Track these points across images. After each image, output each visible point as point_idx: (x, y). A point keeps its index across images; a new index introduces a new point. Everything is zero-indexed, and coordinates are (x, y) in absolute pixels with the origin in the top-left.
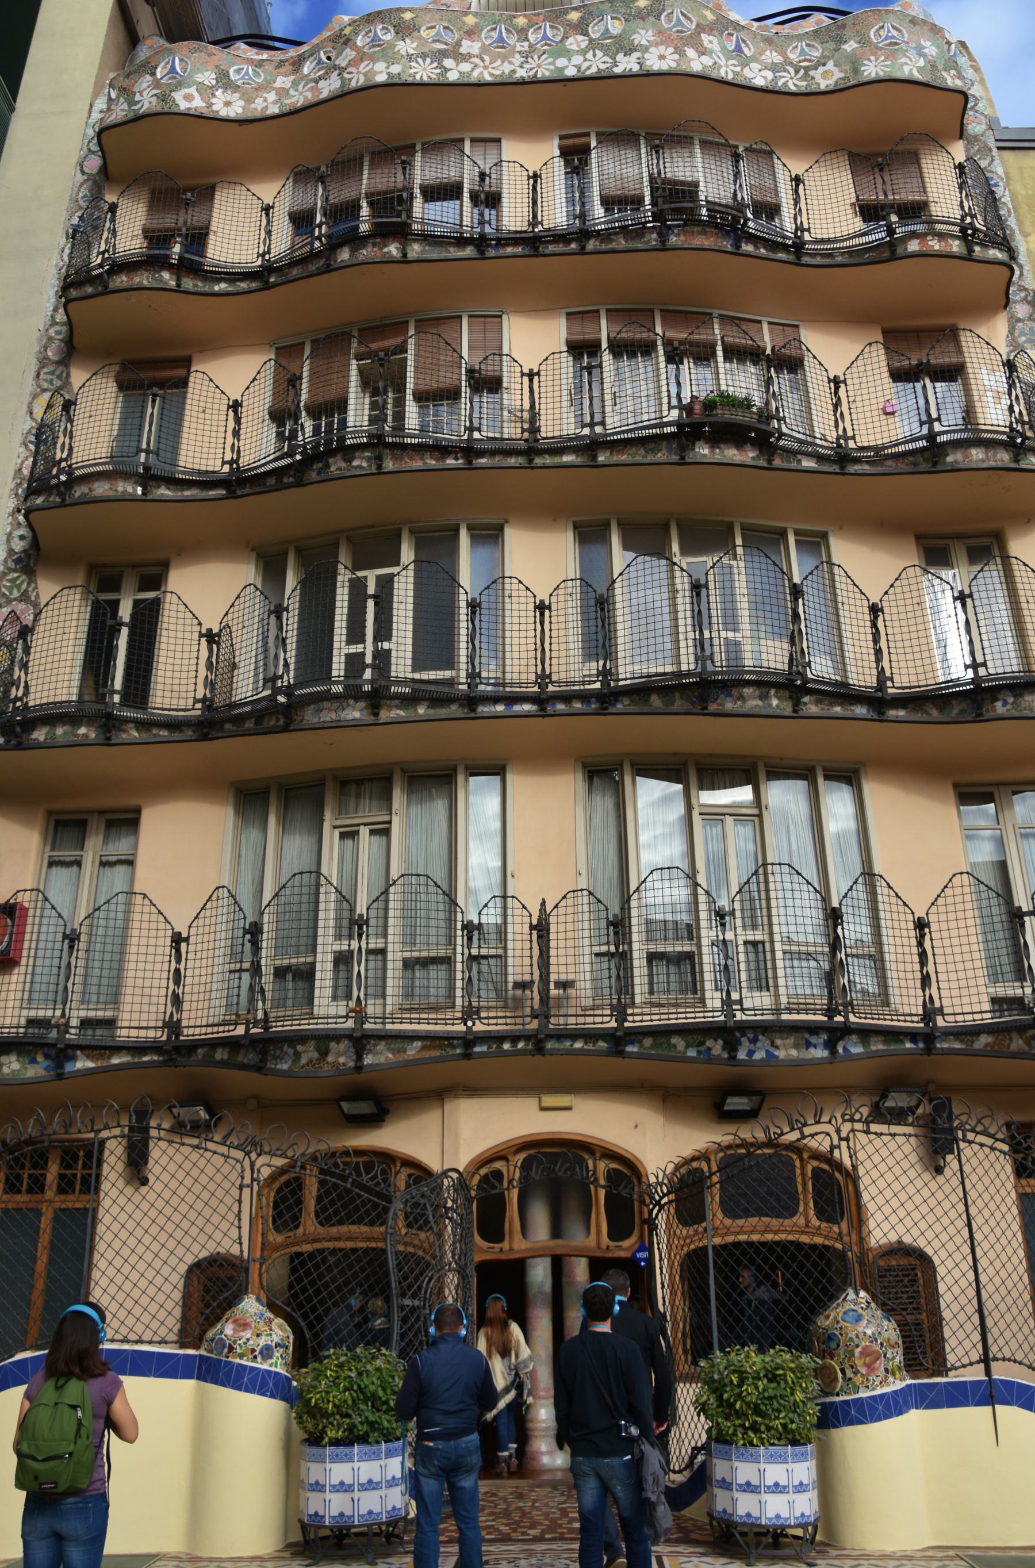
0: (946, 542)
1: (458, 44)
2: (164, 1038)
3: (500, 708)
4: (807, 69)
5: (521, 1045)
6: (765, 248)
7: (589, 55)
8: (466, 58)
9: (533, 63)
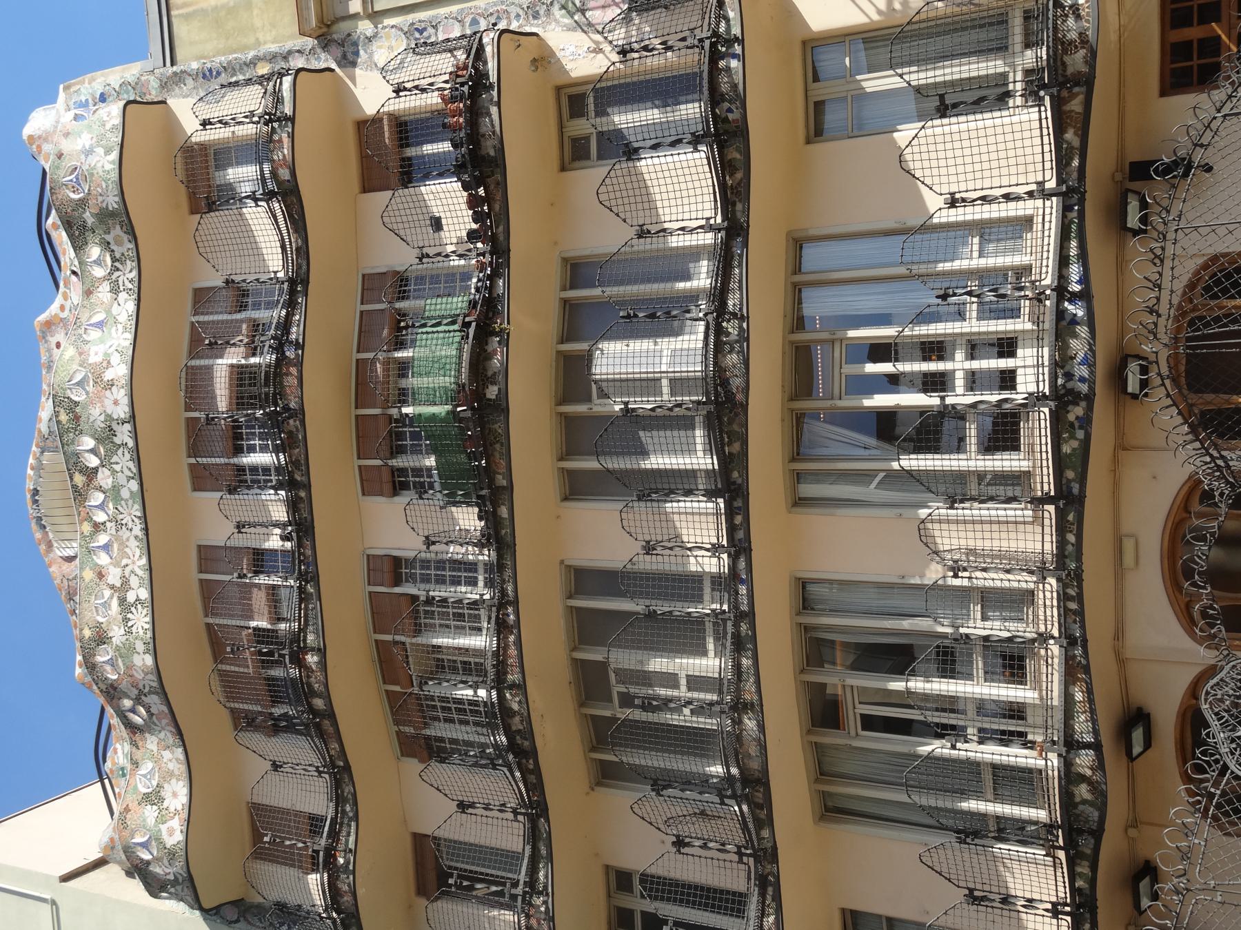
0: (566, 139)
1: (112, 587)
2: (1069, 919)
3: (743, 590)
4: (114, 260)
5: (1072, 592)
6: (294, 315)
9: (127, 520)
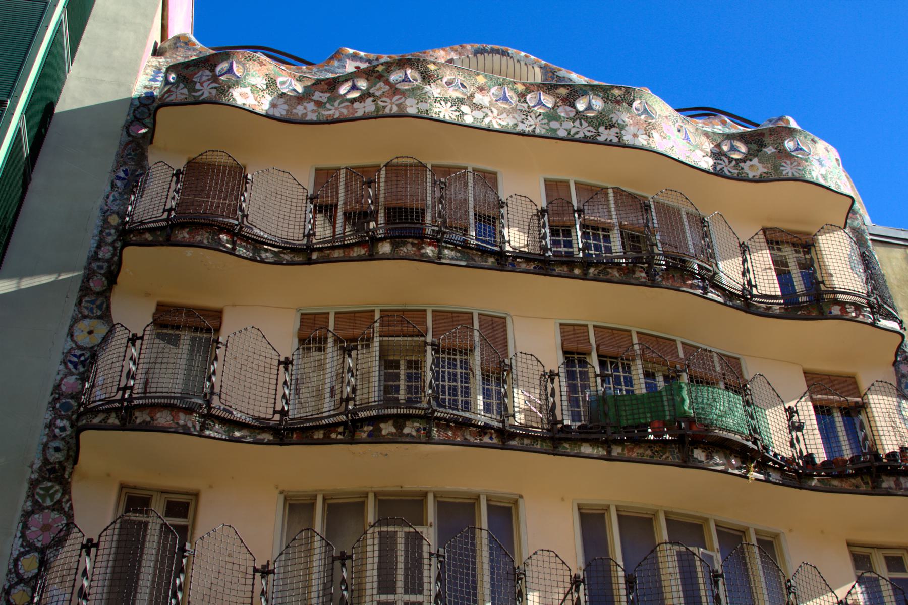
7: (577, 123)
8: (478, 107)
9: (531, 121)
